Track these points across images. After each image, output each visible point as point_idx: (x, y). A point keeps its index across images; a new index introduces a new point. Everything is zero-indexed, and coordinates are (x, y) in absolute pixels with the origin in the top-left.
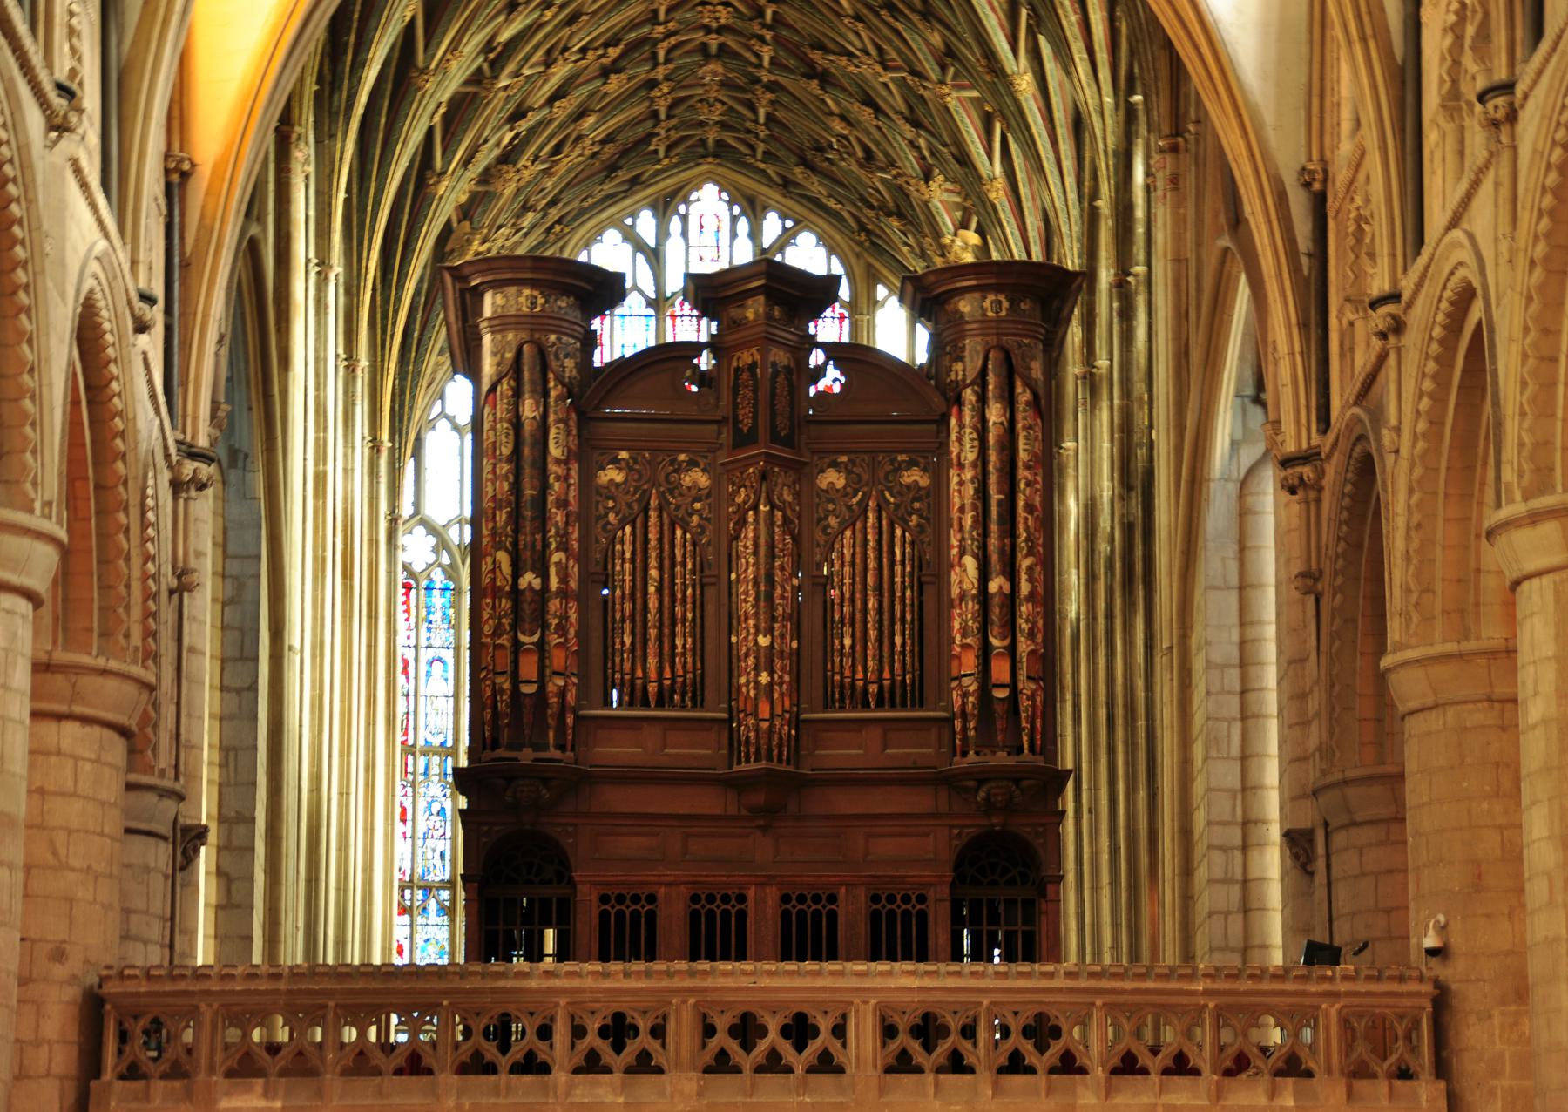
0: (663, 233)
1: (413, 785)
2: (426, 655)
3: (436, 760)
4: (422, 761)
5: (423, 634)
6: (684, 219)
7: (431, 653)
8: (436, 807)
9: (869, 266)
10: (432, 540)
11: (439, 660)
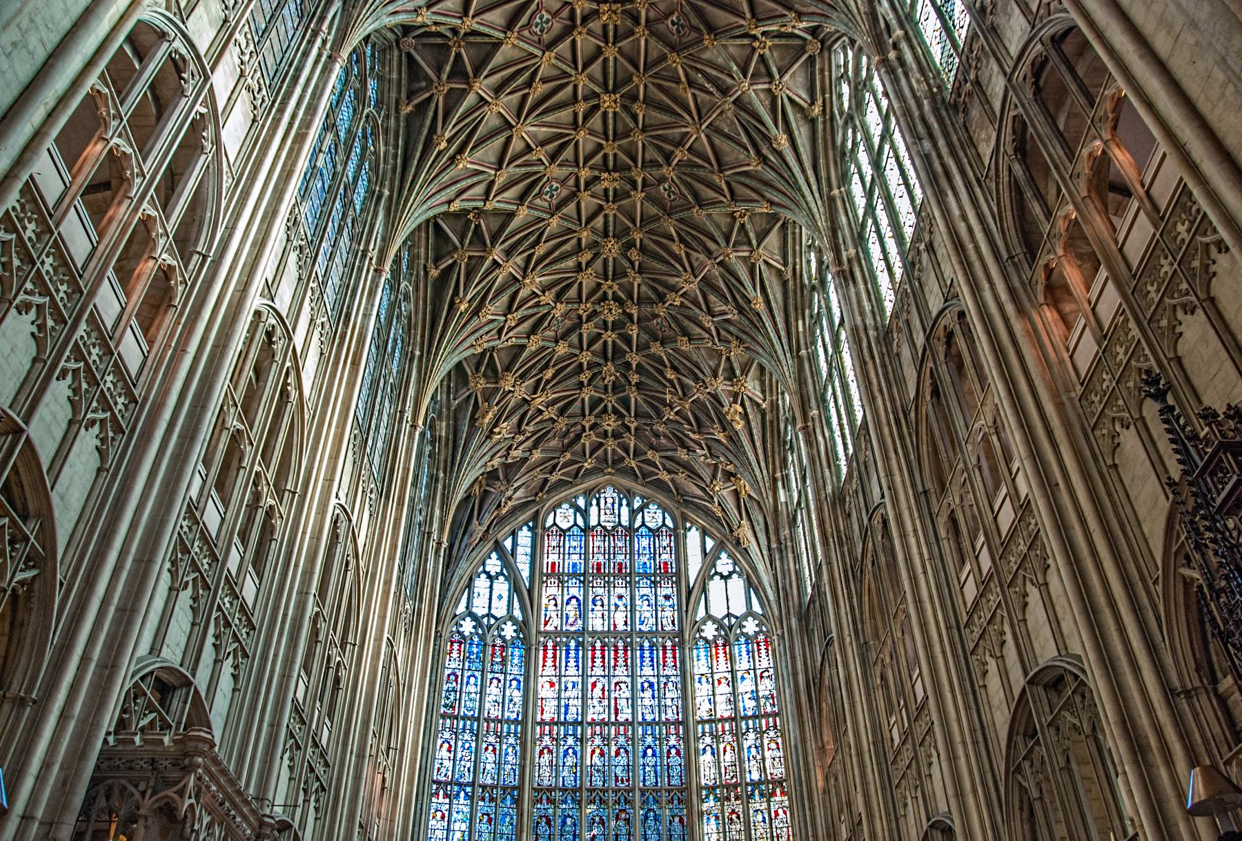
1: (456, 733)
2: (467, 674)
3: (469, 723)
4: (461, 723)
5: (467, 664)
6: (598, 500)
7: (470, 673)
8: (467, 745)
9: (683, 514)
11: (474, 676)
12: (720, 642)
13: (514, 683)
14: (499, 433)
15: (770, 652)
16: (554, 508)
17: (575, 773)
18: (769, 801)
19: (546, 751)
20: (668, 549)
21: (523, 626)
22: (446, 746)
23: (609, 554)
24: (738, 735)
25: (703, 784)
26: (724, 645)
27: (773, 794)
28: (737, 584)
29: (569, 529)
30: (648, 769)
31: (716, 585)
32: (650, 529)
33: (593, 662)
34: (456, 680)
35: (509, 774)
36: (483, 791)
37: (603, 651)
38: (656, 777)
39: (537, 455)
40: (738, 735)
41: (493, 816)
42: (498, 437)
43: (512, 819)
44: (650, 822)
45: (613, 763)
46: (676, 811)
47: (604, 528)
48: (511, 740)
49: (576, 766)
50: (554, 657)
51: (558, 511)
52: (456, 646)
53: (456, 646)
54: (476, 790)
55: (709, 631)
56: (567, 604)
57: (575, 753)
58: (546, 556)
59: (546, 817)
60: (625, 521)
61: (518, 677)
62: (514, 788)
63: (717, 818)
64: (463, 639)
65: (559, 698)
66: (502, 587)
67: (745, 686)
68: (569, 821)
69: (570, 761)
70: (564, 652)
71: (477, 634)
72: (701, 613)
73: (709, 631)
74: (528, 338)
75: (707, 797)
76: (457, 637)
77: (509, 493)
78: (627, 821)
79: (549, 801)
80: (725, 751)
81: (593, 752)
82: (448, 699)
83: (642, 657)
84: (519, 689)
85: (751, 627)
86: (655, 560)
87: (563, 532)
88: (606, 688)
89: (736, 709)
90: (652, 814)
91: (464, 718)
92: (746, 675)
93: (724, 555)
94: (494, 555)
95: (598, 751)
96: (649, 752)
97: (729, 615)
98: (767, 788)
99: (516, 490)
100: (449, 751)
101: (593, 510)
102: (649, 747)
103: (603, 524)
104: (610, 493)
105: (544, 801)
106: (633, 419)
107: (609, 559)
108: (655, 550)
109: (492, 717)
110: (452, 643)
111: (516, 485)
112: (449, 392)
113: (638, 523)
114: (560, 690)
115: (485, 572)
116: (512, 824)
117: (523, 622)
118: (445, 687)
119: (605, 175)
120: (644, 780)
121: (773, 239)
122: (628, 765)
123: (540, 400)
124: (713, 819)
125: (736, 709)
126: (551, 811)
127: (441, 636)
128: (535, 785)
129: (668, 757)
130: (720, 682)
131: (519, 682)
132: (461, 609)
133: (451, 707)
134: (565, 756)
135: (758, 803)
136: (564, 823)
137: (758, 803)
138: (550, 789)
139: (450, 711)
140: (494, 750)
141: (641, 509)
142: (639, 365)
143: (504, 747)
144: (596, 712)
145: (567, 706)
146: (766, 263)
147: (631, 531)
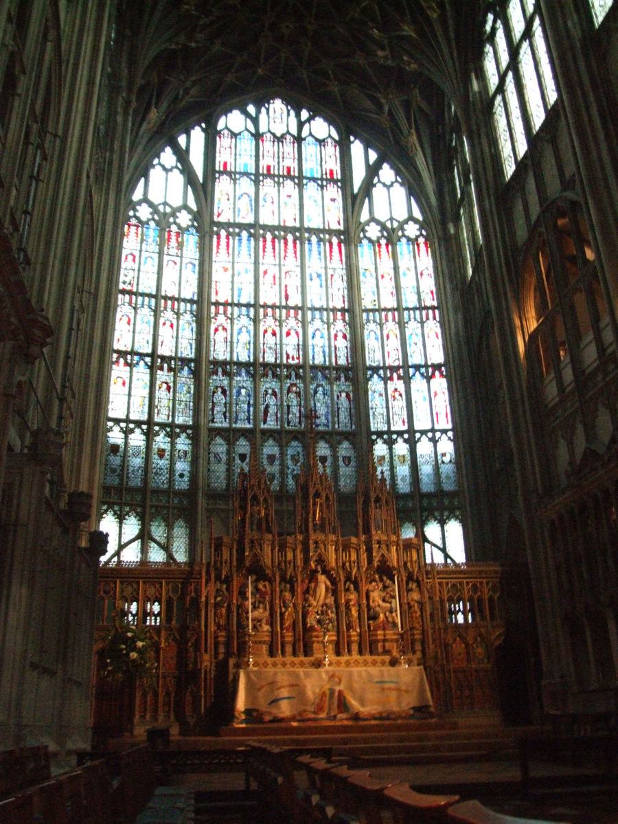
0: (258, 112)
2: (144, 255)
6: (268, 110)
8: (145, 320)
12: (383, 242)
13: (190, 266)
15: (430, 253)
16: (227, 111)
17: (249, 350)
18: (428, 382)
19: (220, 328)
20: (333, 158)
21: (197, 216)
22: (126, 319)
23: (279, 158)
24: (402, 325)
25: (368, 364)
26: (387, 245)
27: (433, 376)
28: (399, 192)
29: (240, 134)
30: (316, 349)
31: (378, 192)
32: (317, 140)
33: (264, 251)
34: (134, 261)
35: (186, 348)
36: (161, 362)
37: (273, 242)
38: (324, 357)
40: (402, 325)
41: (171, 385)
42: (186, 7)
43: (189, 388)
44: (320, 396)
45: (284, 342)
46: (343, 387)
47: (274, 135)
48: (188, 317)
49: (249, 343)
50: (228, 243)
51: (229, 115)
52: (133, 229)
53: (133, 229)
54: (155, 361)
55: (373, 231)
56: (239, 199)
57: (248, 332)
58: (217, 155)
59: (222, 388)
60: (294, 131)
61: (194, 261)
62: (190, 360)
63: (381, 395)
64: (142, 222)
65: (233, 282)
66: (177, 179)
67: (408, 282)
68: (243, 391)
69: (245, 337)
70: (236, 241)
71: (153, 219)
72: (364, 216)
73: (373, 231)
75: (372, 376)
76: (133, 221)
77: (188, 84)
78: (298, 394)
79: (225, 373)
80: (388, 337)
81: (265, 332)
82: (126, 276)
83: (310, 250)
84: (194, 272)
85: (412, 230)
86: (321, 165)
87: (234, 135)
88: (277, 276)
89: (399, 300)
90: (321, 389)
91: (143, 295)
92: (407, 272)
93: (386, 166)
94: (168, 150)
95: (270, 331)
96: (318, 333)
97: (391, 219)
98: (428, 371)
100: (129, 323)
101: (263, 117)
102: (318, 329)
103: (272, 131)
104: (278, 105)
105: (220, 373)
107: (279, 163)
108: (321, 158)
109: (169, 295)
110: (129, 225)
113: (305, 133)
114: (233, 276)
115: (159, 164)
116: (189, 393)
117: (198, 212)
118: (123, 265)
120: (314, 358)
122: (298, 345)
124: (376, 395)
125: (399, 300)
126: (226, 382)
128: (211, 358)
129: (336, 339)
130: (383, 277)
131: (194, 265)
132: (137, 195)
133: (130, 284)
134: (239, 334)
135: (418, 383)
136: (239, 393)
137: (418, 383)
139: (128, 288)
140: (172, 326)
141: (309, 120)
143: (181, 322)
144: (269, 295)
145: (240, 290)
147: (299, 139)
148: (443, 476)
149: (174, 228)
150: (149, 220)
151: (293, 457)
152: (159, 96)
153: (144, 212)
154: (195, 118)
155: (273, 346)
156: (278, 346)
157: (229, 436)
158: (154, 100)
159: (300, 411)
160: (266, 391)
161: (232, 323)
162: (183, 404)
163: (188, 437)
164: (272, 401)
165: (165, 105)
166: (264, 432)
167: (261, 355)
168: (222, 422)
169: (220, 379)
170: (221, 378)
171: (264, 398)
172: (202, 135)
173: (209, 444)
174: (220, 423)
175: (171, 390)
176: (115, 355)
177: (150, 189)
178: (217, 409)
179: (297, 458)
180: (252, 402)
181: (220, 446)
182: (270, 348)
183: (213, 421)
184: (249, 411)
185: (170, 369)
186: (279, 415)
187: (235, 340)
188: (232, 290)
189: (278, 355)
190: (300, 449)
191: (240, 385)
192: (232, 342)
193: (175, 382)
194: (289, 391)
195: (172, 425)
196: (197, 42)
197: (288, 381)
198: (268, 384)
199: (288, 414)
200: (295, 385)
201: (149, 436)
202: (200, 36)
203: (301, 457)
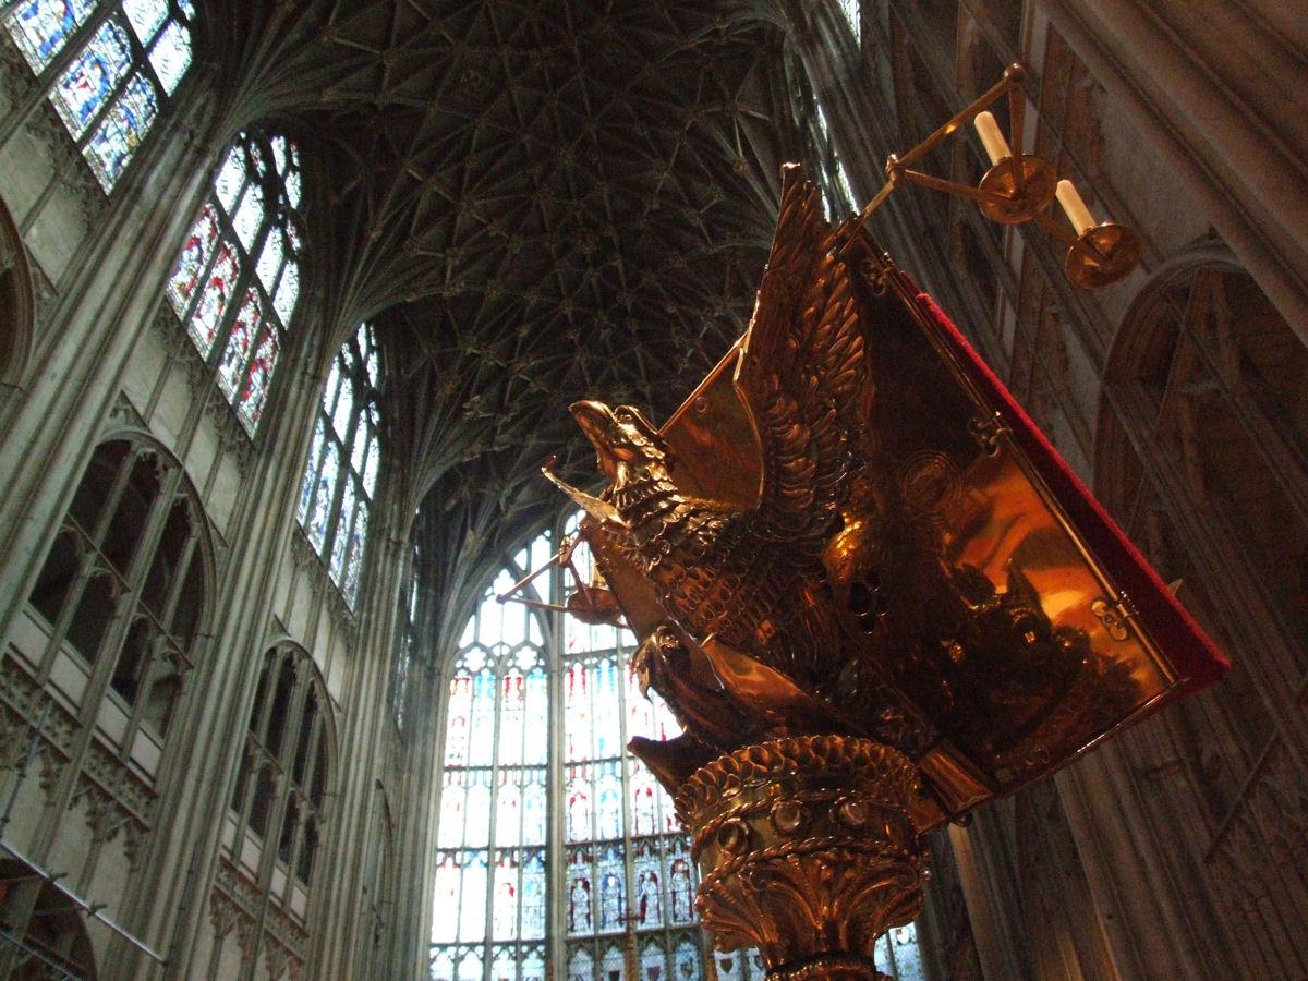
10: (484, 655)
14: (471, 409)
21: (543, 652)
39: (533, 441)
52: (462, 683)
53: (462, 683)
54: (494, 854)
62: (540, 848)
68: (612, 881)
74: (485, 283)
78: (686, 873)
79: (588, 859)
94: (505, 573)
99: (517, 489)
105: (580, 860)
106: (644, 382)
111: (512, 485)
112: (398, 369)
114: (593, 722)
116: (539, 893)
117: (543, 647)
119: (533, 53)
121: (749, 85)
123: (522, 365)
126: (588, 872)
127: (440, 674)
128: (567, 841)
136: (606, 884)
138: (586, 845)
142: (634, 305)
146: (747, 117)
148: (901, 965)
149: (514, 674)
150: (481, 669)
151: (684, 966)
152: (475, 512)
153: (475, 660)
154: (533, 528)
155: (649, 811)
156: (655, 810)
157: (594, 948)
158: (469, 521)
159: (690, 897)
160: (643, 876)
161: (593, 787)
162: (531, 910)
163: (540, 956)
164: (650, 889)
165: (482, 523)
166: (641, 935)
167: (633, 826)
168: (584, 930)
169: (581, 868)
170: (582, 866)
171: (640, 885)
172: (548, 544)
173: (568, 962)
174: (583, 930)
175: (516, 893)
176: (440, 856)
177: (481, 629)
178: (578, 911)
179: (689, 967)
180: (623, 895)
181: (583, 964)
182: (645, 814)
183: (572, 929)
184: (620, 908)
185: (514, 864)
186: (661, 908)
187: (598, 811)
188: (592, 742)
189: (656, 823)
190: (693, 954)
191: (607, 873)
192: (594, 814)
193: (520, 882)
194: (673, 871)
195: (517, 943)
196: (500, 445)
197: (672, 857)
198: (646, 865)
199: (674, 903)
200: (681, 861)
201: (488, 960)
202: (505, 437)
203: (695, 964)
